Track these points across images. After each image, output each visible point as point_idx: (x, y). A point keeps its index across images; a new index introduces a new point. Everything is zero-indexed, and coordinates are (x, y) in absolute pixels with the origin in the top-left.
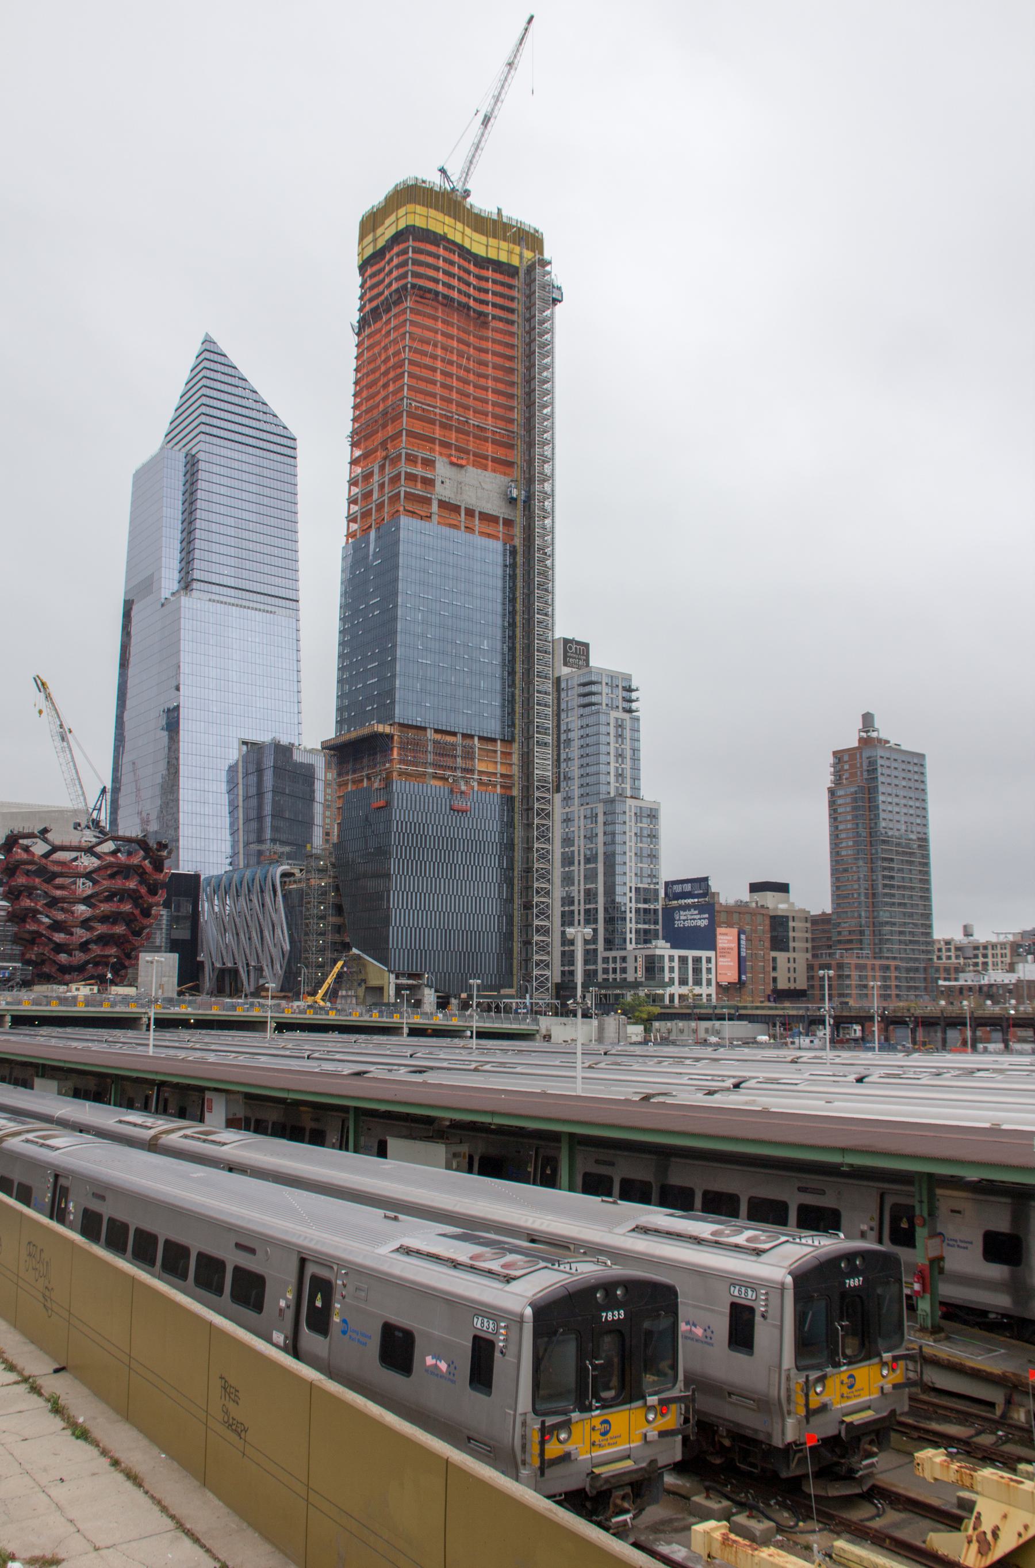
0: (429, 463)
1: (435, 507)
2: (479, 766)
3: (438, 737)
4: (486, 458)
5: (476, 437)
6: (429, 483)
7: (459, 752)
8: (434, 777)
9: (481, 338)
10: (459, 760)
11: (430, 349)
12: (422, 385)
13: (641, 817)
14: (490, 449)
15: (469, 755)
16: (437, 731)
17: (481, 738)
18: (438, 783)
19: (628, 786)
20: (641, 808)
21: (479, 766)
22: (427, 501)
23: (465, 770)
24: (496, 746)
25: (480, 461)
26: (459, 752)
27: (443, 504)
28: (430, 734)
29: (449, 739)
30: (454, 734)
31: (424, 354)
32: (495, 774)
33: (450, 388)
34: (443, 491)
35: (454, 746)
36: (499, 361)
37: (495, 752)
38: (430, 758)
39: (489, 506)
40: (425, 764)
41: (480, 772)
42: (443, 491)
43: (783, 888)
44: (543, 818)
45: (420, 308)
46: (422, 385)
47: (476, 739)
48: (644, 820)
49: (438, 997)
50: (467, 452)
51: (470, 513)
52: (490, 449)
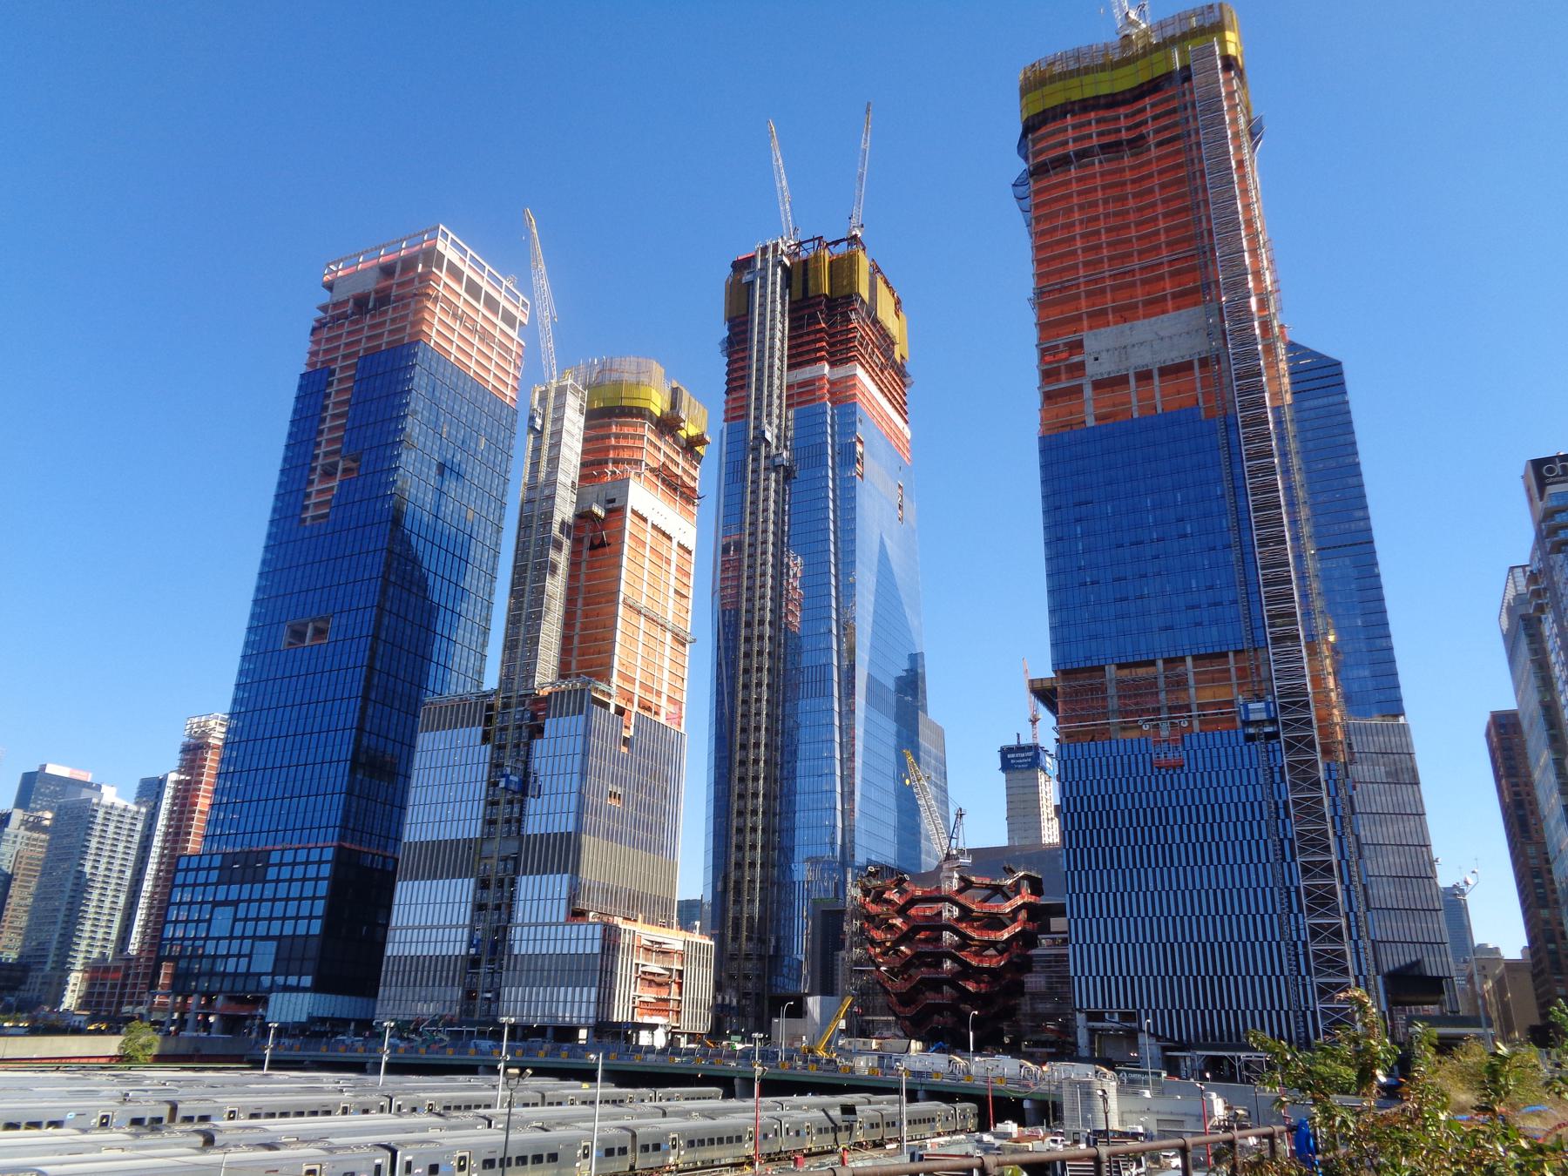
0: (1077, 346)
1: (1088, 392)
2: (1193, 695)
3: (1126, 672)
4: (1164, 298)
5: (1144, 282)
6: (1081, 366)
7: (1161, 682)
8: (1124, 729)
9: (1142, 165)
10: (1162, 696)
11: (1061, 222)
12: (1057, 266)
14: (1168, 286)
15: (1179, 683)
16: (1120, 666)
17: (1196, 658)
18: (1134, 734)
22: (1078, 390)
23: (1171, 709)
25: (1155, 306)
26: (1161, 682)
27: (1098, 385)
28: (1111, 670)
29: (1141, 672)
30: (1153, 663)
31: (1054, 230)
33: (1098, 248)
34: (1094, 370)
35: (1152, 683)
36: (1166, 178)
39: (1174, 354)
40: (1105, 715)
41: (1201, 706)
42: (1094, 370)
44: (1300, 751)
45: (1044, 183)
46: (1057, 266)
47: (1189, 660)
49: (1165, 1049)
50: (1134, 306)
51: (1144, 376)
52: (1168, 286)
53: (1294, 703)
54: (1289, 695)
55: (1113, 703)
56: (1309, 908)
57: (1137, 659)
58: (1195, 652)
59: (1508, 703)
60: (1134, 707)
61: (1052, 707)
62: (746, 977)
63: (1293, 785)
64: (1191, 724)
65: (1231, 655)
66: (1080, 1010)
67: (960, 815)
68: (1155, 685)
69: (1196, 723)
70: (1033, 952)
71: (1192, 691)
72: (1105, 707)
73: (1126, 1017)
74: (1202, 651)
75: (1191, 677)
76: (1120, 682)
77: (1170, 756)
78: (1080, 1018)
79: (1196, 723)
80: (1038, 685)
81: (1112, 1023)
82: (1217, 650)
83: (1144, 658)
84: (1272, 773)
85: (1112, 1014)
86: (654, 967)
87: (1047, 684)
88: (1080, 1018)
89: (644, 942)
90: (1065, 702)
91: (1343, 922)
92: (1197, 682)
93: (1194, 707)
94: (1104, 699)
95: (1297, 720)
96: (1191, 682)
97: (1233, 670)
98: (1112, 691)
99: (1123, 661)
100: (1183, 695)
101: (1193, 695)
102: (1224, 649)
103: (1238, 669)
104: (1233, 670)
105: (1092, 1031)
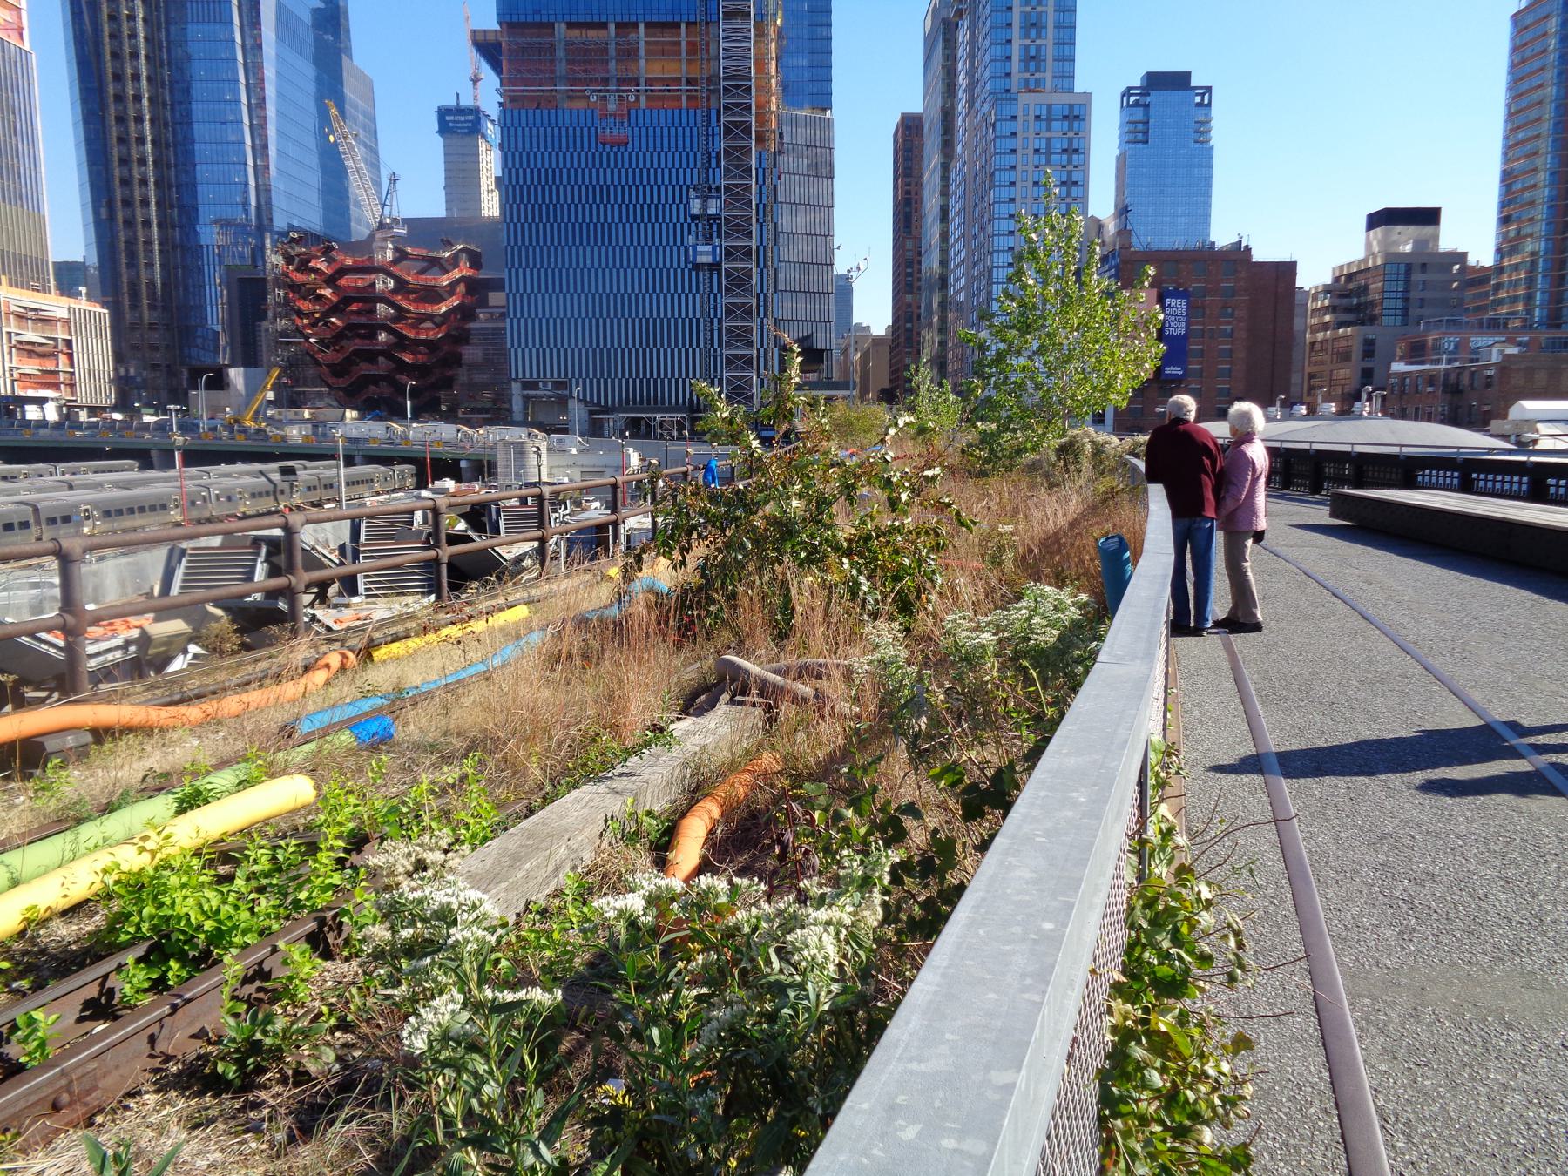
3: (576, 33)
8: (571, 98)
10: (612, 65)
13: (1049, 120)
15: (629, 53)
16: (570, 25)
17: (648, 25)
18: (579, 105)
19: (1049, 75)
20: (1049, 106)
21: (646, 68)
23: (621, 81)
24: (679, 35)
28: (561, 29)
29: (592, 34)
30: (603, 26)
32: (677, 81)
37: (679, 43)
38: (562, 68)
40: (553, 81)
41: (649, 81)
43: (1429, 217)
47: (641, 27)
48: (1056, 125)
49: (591, 413)
53: (737, 87)
54: (733, 78)
55: (562, 68)
56: (727, 289)
57: (589, 19)
58: (648, 19)
59: (916, 106)
60: (582, 75)
61: (496, 66)
62: (153, 348)
63: (727, 171)
64: (638, 98)
65: (683, 26)
66: (516, 380)
67: (394, 180)
68: (606, 51)
69: (643, 99)
70: (472, 325)
71: (642, 63)
72: (553, 71)
73: (558, 385)
74: (655, 19)
75: (642, 45)
76: (569, 44)
77: (615, 131)
78: (516, 388)
79: (643, 99)
80: (480, 38)
81: (545, 391)
82: (670, 19)
83: (596, 19)
84: (709, 158)
85: (545, 384)
86: (32, 335)
87: (491, 38)
88: (516, 388)
89: (13, 308)
90: (509, 61)
91: (754, 301)
92: (648, 52)
93: (642, 81)
94: (552, 62)
95: (737, 105)
96: (642, 52)
97: (683, 44)
98: (560, 53)
99: (574, 19)
100: (633, 66)
101: (646, 68)
102: (677, 19)
103: (688, 43)
104: (683, 44)
105: (526, 399)
